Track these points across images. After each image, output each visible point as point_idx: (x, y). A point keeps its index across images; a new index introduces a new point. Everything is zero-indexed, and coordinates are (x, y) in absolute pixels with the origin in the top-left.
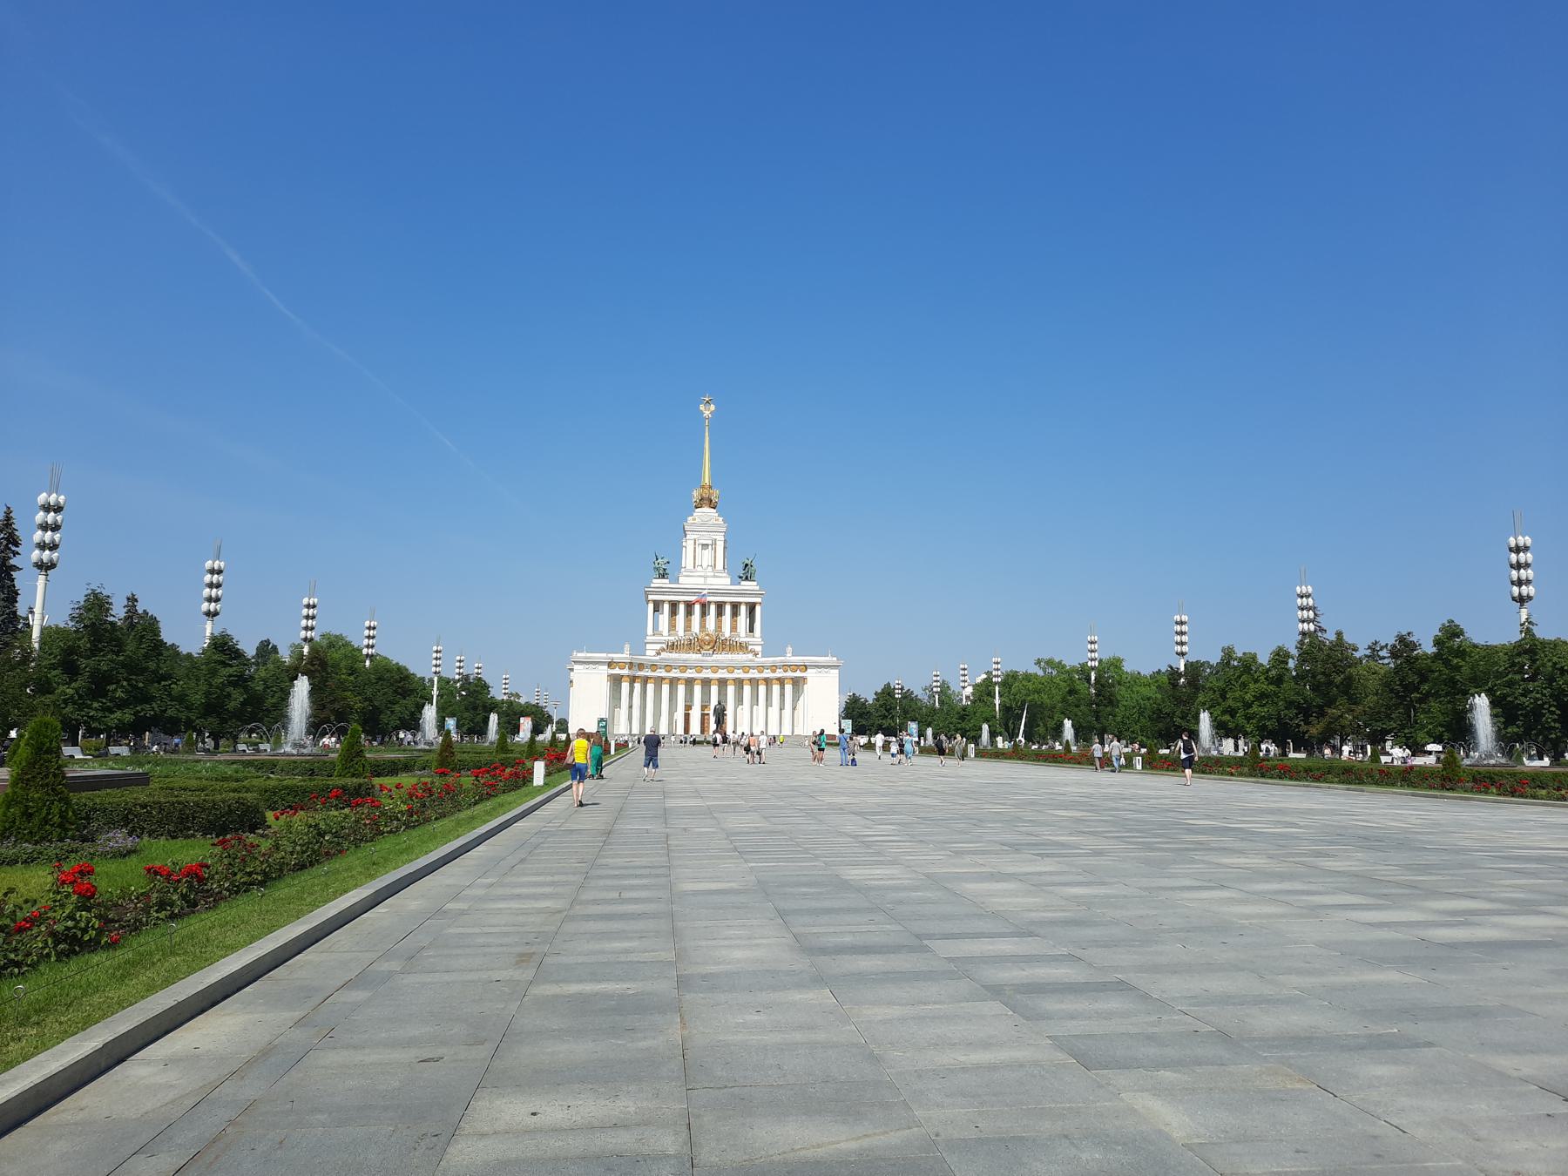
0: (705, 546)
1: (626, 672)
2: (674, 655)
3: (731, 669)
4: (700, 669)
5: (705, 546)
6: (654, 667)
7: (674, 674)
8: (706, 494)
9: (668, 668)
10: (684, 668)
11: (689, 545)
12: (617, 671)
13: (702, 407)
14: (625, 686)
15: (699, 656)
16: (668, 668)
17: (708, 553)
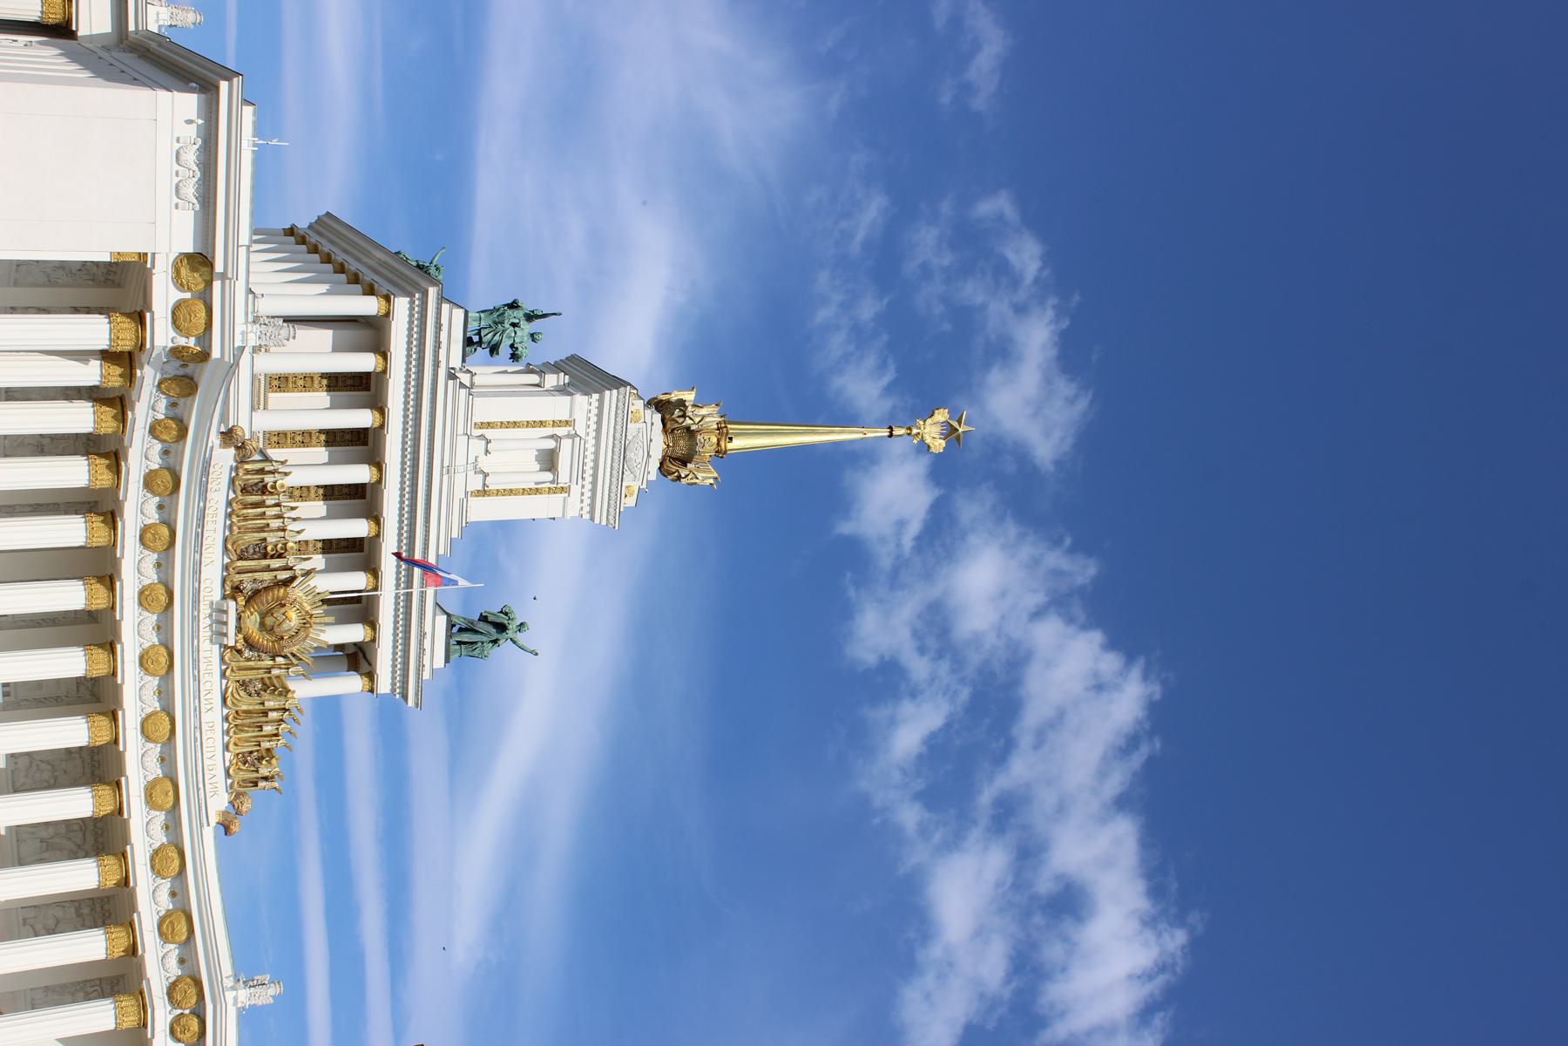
0: (549, 461)
1: (162, 334)
2: (219, 495)
3: (162, 727)
4: (159, 598)
5: (549, 461)
6: (173, 430)
7: (137, 508)
8: (707, 443)
9: (165, 483)
10: (160, 538)
11: (557, 407)
12: (164, 294)
13: (941, 416)
14: (95, 331)
15: (212, 588)
16: (165, 483)
17: (535, 475)
